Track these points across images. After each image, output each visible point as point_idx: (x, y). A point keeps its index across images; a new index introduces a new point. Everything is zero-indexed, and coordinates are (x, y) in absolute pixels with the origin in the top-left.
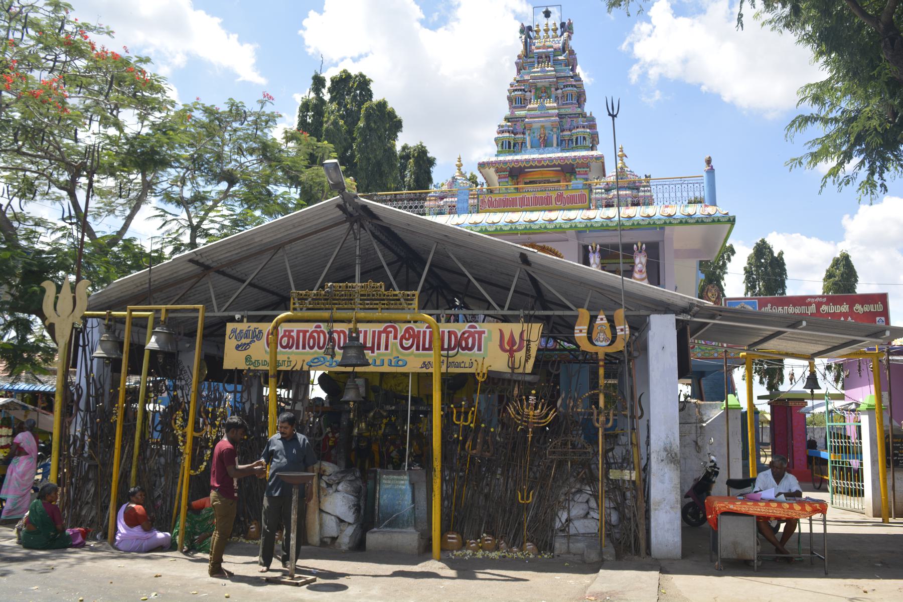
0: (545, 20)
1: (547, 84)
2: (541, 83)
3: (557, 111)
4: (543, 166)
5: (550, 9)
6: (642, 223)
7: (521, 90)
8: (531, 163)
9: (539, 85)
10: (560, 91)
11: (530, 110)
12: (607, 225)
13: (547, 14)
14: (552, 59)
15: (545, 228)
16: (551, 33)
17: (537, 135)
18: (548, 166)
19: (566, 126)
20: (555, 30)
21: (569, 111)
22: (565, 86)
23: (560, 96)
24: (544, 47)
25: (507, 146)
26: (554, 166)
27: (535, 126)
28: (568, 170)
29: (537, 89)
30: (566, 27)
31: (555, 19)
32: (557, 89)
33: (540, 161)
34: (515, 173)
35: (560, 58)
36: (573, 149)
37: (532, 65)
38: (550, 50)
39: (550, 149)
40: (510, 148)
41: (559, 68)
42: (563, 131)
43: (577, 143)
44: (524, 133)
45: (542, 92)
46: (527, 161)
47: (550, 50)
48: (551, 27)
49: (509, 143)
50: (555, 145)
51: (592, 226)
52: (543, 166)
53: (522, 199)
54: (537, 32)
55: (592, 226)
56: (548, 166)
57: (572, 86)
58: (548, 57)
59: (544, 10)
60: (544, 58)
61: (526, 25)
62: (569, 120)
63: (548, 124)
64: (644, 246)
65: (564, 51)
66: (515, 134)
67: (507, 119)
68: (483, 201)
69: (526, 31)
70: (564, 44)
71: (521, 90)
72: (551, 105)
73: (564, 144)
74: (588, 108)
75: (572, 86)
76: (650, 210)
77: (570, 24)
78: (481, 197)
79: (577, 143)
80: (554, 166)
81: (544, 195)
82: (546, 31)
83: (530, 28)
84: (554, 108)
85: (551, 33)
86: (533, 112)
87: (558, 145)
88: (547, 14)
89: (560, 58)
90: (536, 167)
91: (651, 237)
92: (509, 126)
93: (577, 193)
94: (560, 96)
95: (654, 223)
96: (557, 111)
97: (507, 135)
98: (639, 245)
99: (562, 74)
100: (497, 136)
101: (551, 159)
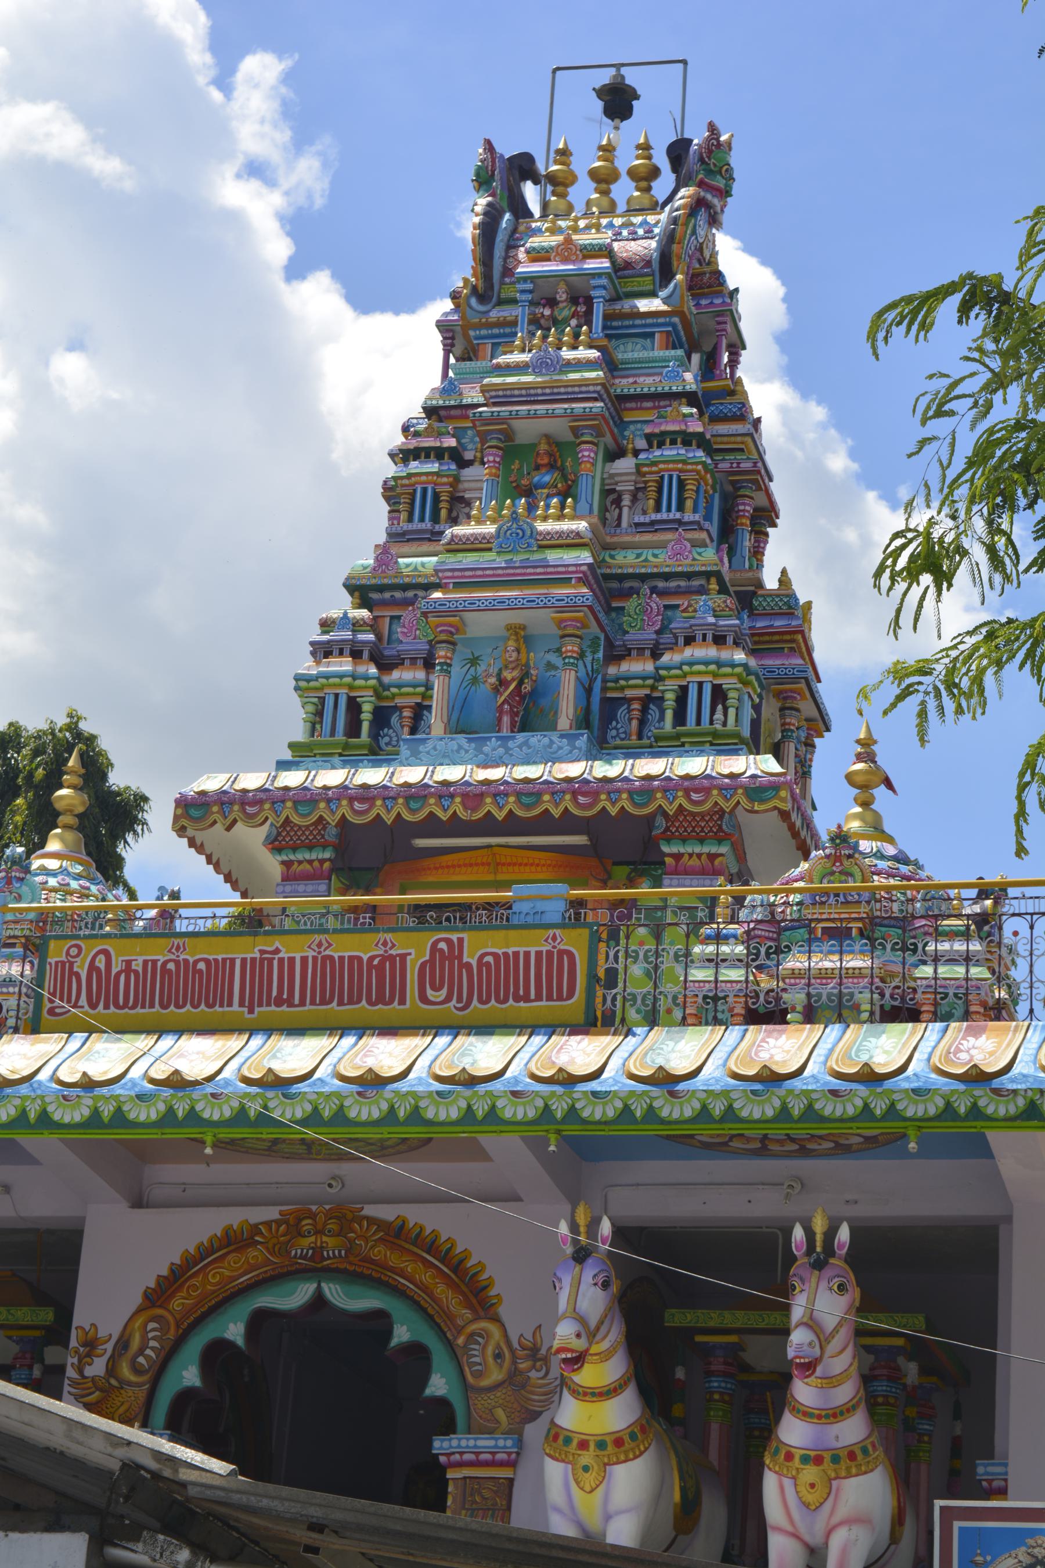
0: (607, 132)
1: (560, 428)
2: (531, 425)
3: (585, 557)
4: (488, 826)
5: (632, 77)
6: (828, 1108)
7: (439, 454)
8: (432, 806)
9: (526, 431)
10: (625, 465)
11: (459, 546)
12: (651, 1114)
13: (618, 101)
14: (599, 310)
15: (340, 1117)
16: (624, 190)
17: (488, 667)
18: (513, 825)
19: (643, 634)
20: (646, 177)
21: (660, 560)
22: (656, 440)
23: (626, 487)
24: (568, 251)
25: (353, 722)
26: (544, 824)
27: (482, 625)
28: (622, 843)
29: (511, 450)
30: (703, 169)
31: (652, 125)
32: (615, 454)
33: (473, 794)
34: (364, 849)
35: (644, 305)
36: (657, 748)
37: (503, 335)
38: (592, 264)
39: (536, 739)
40: (353, 729)
41: (629, 352)
42: (616, 654)
43: (680, 717)
44: (429, 665)
45: (535, 467)
46: (414, 793)
47: (592, 264)
48: (627, 159)
49: (354, 707)
50: (564, 723)
51: (572, 1112)
52: (488, 826)
53: (258, 968)
54: (559, 183)
55: (572, 1112)
56: (513, 825)
57: (687, 439)
58: (581, 299)
59: (605, 77)
60: (565, 303)
61: (507, 149)
62: (657, 603)
63: (541, 621)
64: (844, 1234)
65: (666, 274)
66: (385, 665)
67: (360, 591)
68: (66, 970)
69: (506, 177)
70: (670, 239)
71: (439, 454)
72: (566, 526)
73: (605, 724)
74: (781, 557)
75: (687, 439)
76: (984, 1047)
77: (716, 145)
78: (56, 953)
79: (680, 717)
80: (544, 824)
81: (363, 947)
82: (603, 179)
83: (523, 167)
84: (573, 542)
85: (624, 190)
86: (469, 560)
87: (584, 721)
88: (618, 101)
89: (644, 305)
90: (456, 827)
91: (914, 1192)
92: (357, 626)
93: (534, 944)
94: (626, 487)
95: (892, 1112)
96: (585, 557)
97: (343, 665)
98: (819, 1226)
99: (647, 383)
100: (308, 666)
101: (528, 790)
